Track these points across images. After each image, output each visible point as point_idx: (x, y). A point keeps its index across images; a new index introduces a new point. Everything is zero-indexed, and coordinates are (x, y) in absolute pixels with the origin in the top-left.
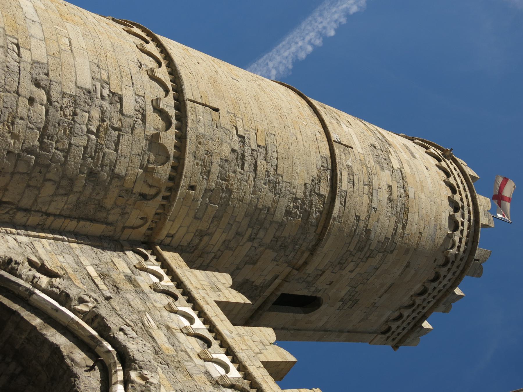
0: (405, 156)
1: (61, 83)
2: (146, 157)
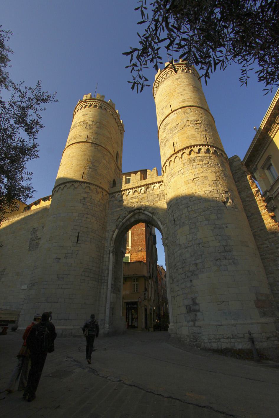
0: (87, 118)
1: (82, 211)
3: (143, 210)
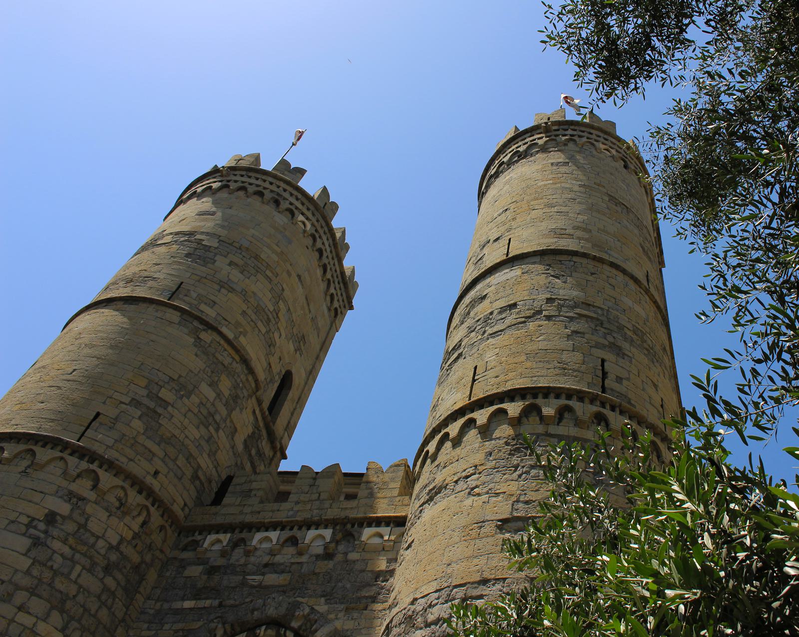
0: (208, 225)
1: (16, 571)
2: (115, 510)
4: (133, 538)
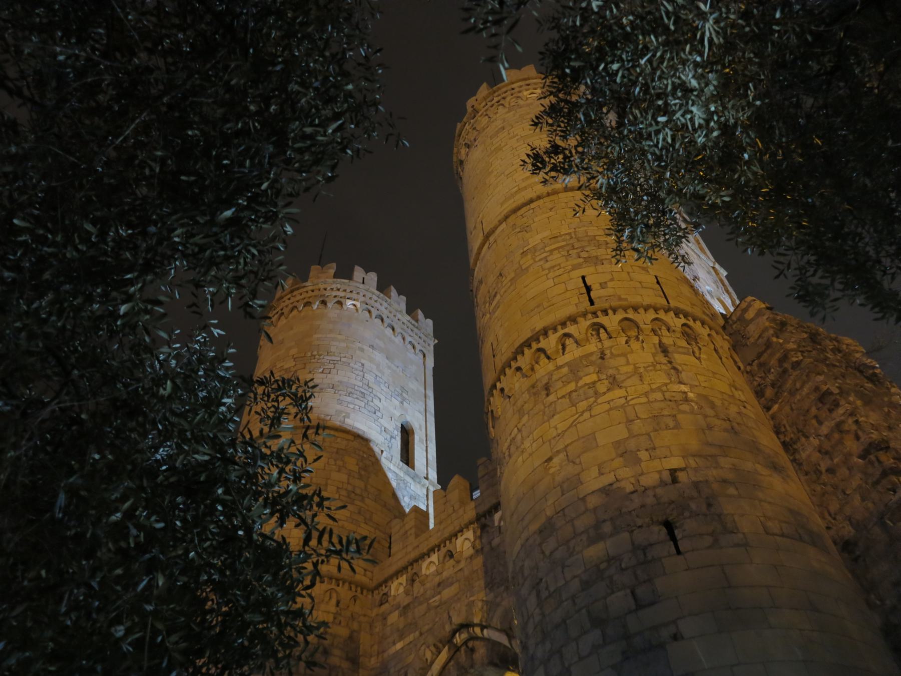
3: (477, 625)
4: (335, 618)
